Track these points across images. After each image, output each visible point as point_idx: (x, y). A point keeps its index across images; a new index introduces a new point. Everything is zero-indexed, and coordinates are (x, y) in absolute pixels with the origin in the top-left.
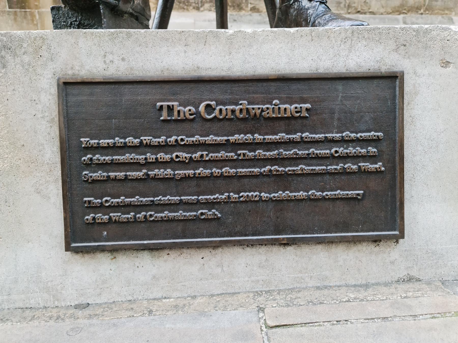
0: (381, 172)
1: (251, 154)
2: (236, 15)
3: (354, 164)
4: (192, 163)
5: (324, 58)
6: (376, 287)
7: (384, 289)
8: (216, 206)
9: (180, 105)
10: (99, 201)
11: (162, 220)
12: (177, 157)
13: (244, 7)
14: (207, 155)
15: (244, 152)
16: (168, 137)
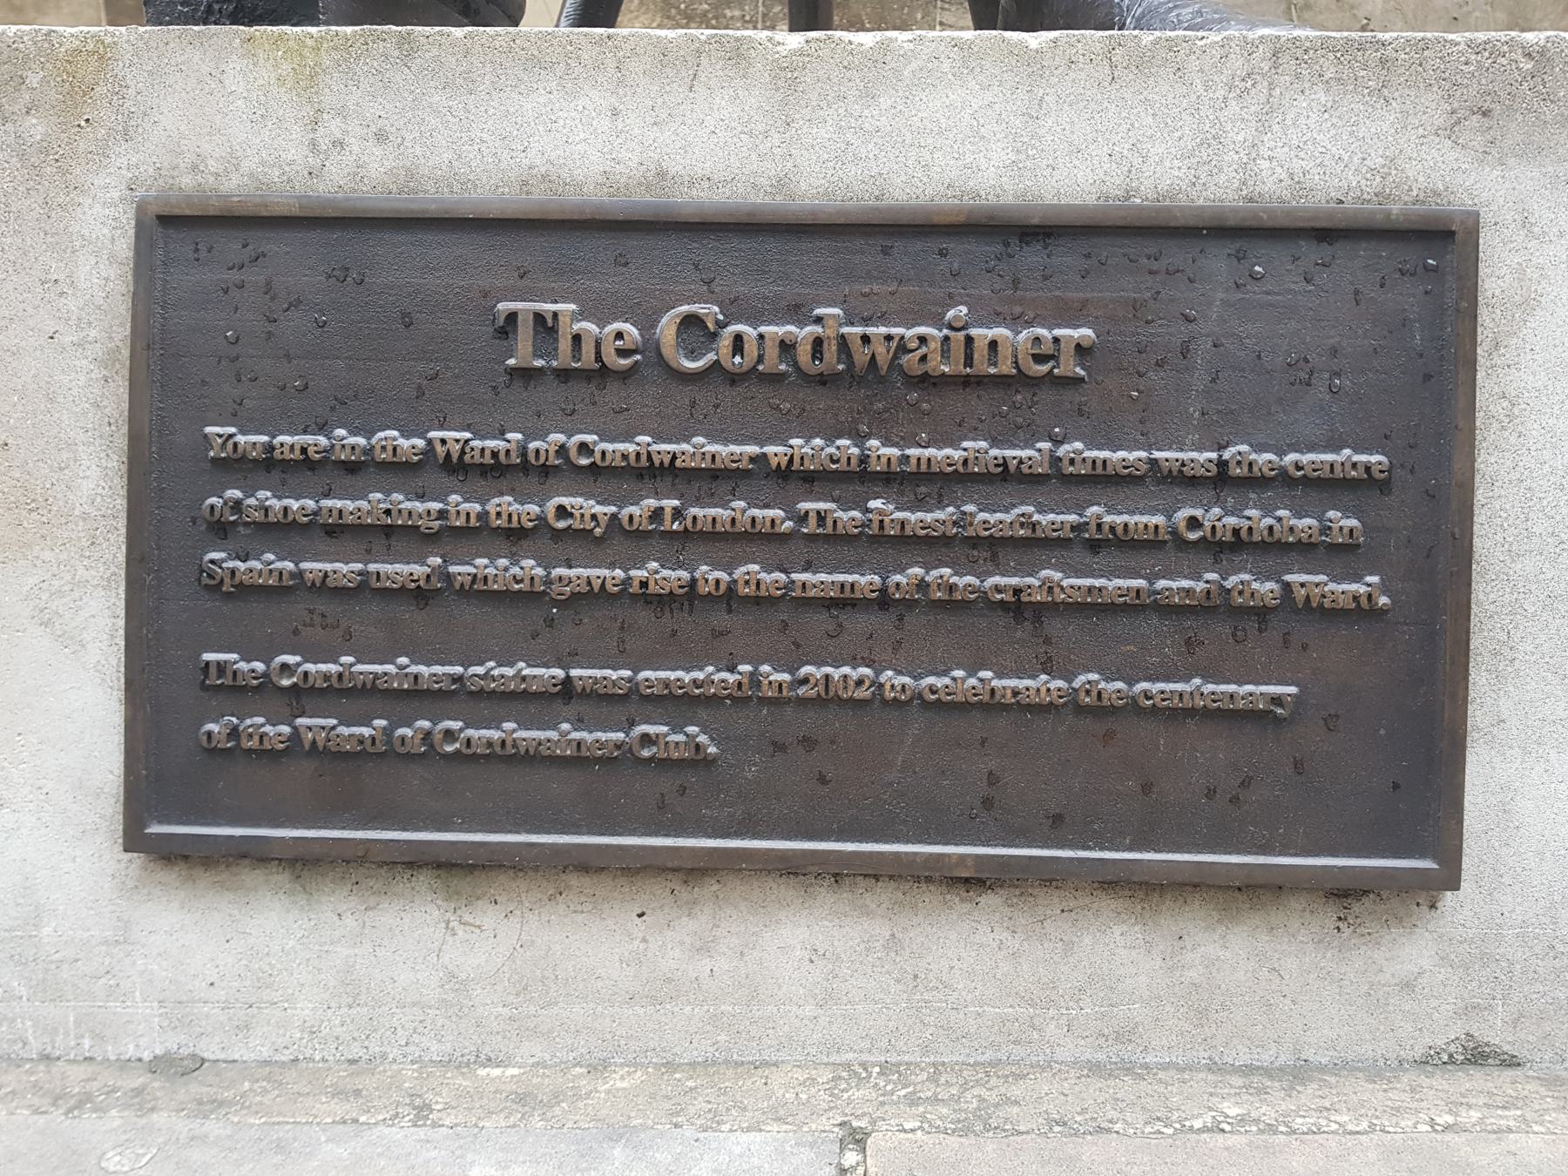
0: (1376, 613)
1: (848, 517)
3: (1263, 576)
5: (1160, 149)
6: (1333, 1080)
7: (1367, 1091)
8: (703, 714)
9: (582, 315)
12: (562, 512)
14: (678, 514)
15: (822, 506)
16: (529, 437)
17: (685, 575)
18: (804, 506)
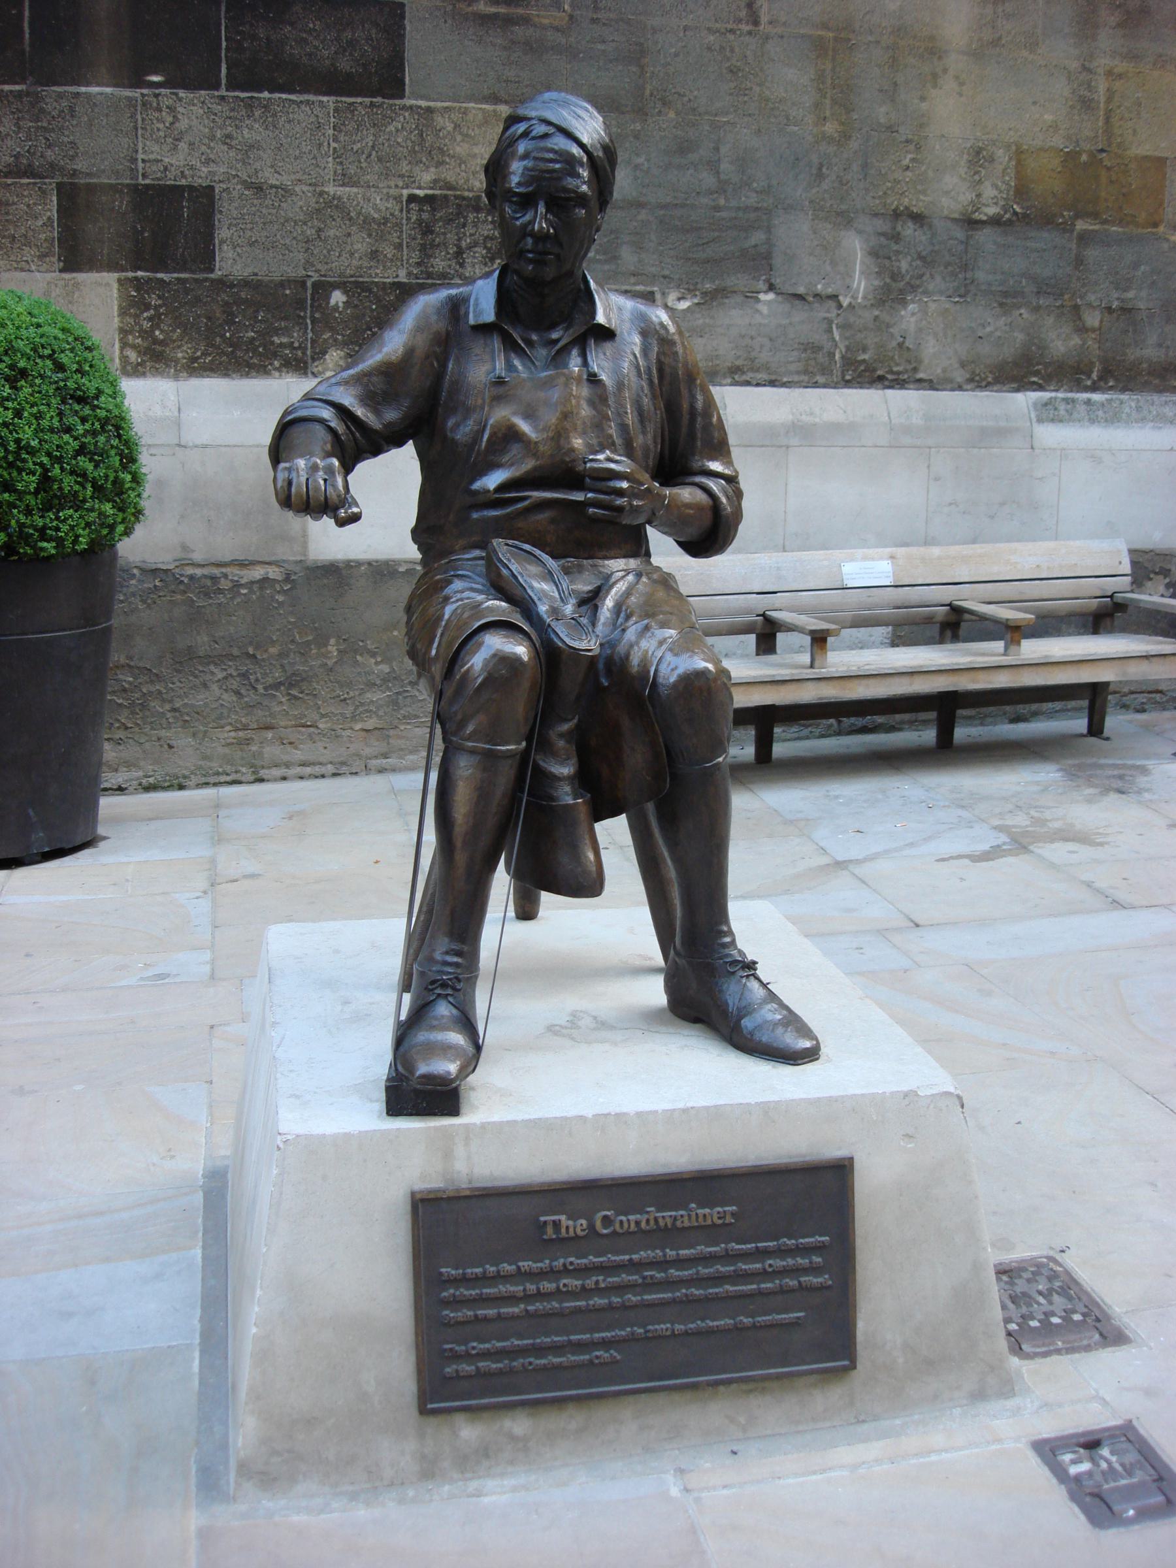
0: (829, 1287)
1: (659, 1275)
4: (585, 1292)
10: (463, 1348)
11: (544, 1368)
14: (604, 1280)
16: (552, 1260)
17: (606, 1301)
18: (646, 1273)
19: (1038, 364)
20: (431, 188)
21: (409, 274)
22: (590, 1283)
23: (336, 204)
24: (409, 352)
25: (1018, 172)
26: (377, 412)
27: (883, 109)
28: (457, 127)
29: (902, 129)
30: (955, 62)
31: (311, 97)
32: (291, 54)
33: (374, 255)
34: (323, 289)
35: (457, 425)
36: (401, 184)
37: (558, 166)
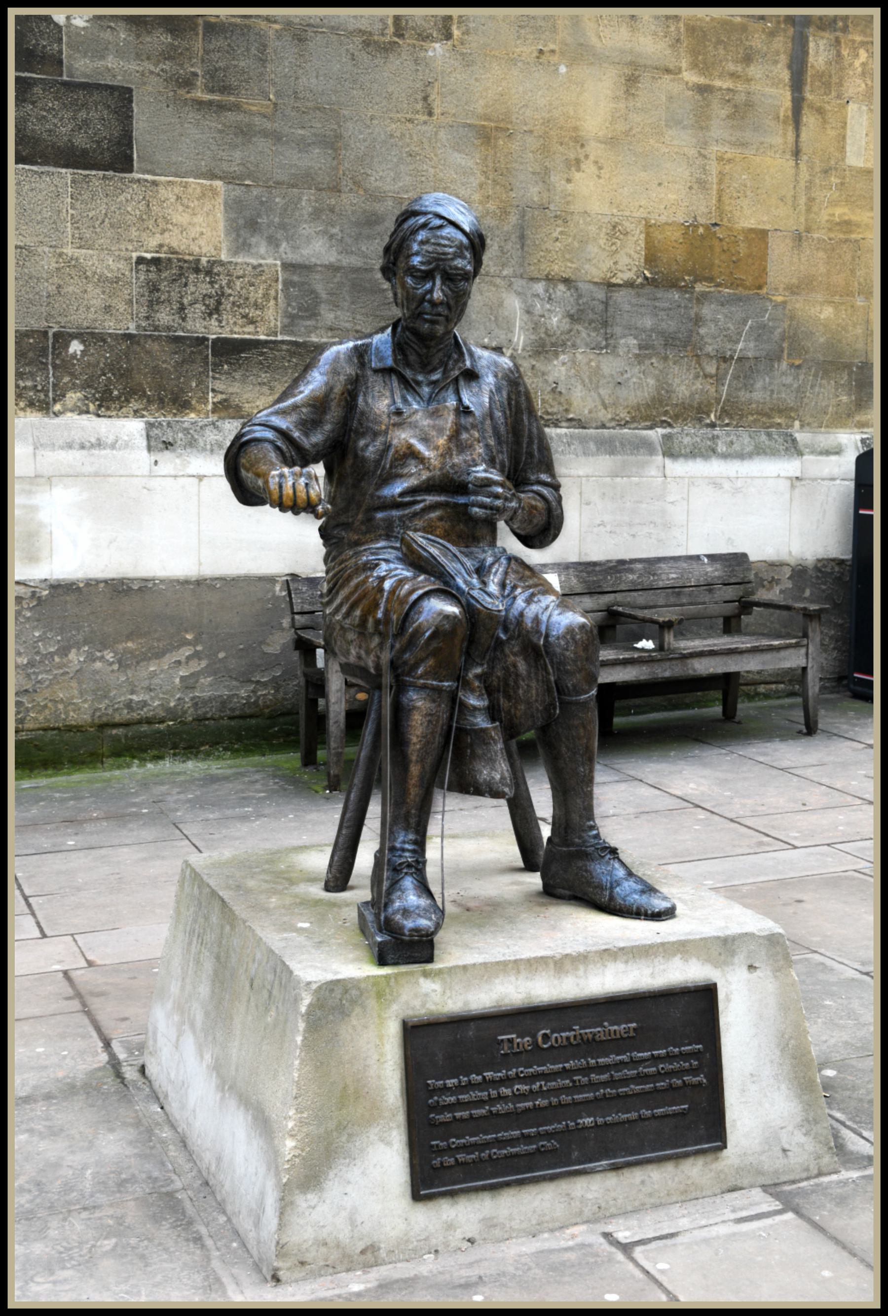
1: (585, 1080)
2: (169, 424)
4: (531, 1095)
13: (193, 402)
19: (667, 405)
20: (157, 252)
21: (138, 327)
22: (536, 1087)
23: (73, 263)
24: (330, 389)
25: (647, 243)
26: (306, 435)
27: (536, 189)
28: (178, 198)
29: (552, 207)
30: (594, 150)
31: (51, 169)
32: (33, 130)
33: (108, 309)
34: (62, 338)
35: (367, 446)
36: (130, 248)
37: (451, 250)
